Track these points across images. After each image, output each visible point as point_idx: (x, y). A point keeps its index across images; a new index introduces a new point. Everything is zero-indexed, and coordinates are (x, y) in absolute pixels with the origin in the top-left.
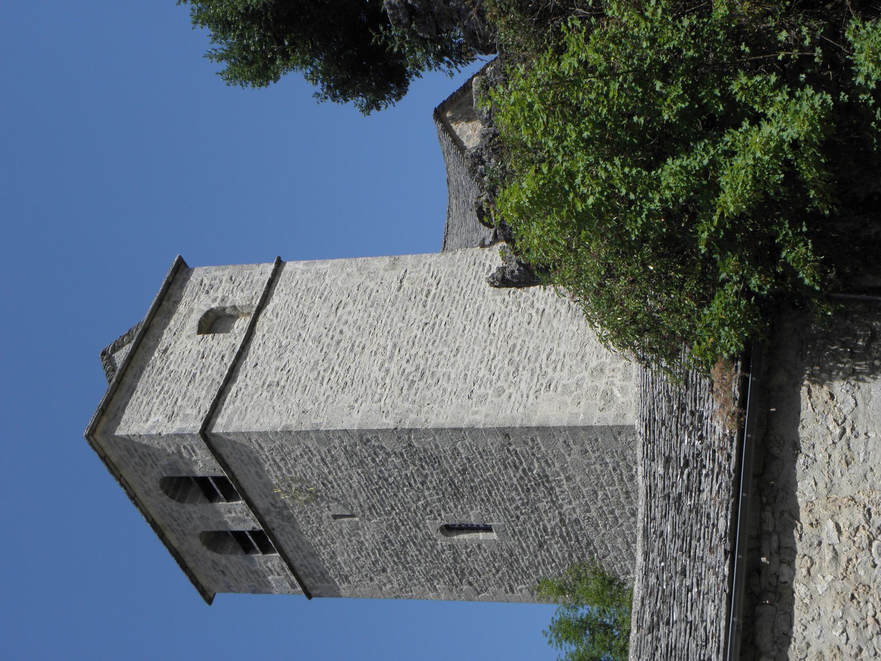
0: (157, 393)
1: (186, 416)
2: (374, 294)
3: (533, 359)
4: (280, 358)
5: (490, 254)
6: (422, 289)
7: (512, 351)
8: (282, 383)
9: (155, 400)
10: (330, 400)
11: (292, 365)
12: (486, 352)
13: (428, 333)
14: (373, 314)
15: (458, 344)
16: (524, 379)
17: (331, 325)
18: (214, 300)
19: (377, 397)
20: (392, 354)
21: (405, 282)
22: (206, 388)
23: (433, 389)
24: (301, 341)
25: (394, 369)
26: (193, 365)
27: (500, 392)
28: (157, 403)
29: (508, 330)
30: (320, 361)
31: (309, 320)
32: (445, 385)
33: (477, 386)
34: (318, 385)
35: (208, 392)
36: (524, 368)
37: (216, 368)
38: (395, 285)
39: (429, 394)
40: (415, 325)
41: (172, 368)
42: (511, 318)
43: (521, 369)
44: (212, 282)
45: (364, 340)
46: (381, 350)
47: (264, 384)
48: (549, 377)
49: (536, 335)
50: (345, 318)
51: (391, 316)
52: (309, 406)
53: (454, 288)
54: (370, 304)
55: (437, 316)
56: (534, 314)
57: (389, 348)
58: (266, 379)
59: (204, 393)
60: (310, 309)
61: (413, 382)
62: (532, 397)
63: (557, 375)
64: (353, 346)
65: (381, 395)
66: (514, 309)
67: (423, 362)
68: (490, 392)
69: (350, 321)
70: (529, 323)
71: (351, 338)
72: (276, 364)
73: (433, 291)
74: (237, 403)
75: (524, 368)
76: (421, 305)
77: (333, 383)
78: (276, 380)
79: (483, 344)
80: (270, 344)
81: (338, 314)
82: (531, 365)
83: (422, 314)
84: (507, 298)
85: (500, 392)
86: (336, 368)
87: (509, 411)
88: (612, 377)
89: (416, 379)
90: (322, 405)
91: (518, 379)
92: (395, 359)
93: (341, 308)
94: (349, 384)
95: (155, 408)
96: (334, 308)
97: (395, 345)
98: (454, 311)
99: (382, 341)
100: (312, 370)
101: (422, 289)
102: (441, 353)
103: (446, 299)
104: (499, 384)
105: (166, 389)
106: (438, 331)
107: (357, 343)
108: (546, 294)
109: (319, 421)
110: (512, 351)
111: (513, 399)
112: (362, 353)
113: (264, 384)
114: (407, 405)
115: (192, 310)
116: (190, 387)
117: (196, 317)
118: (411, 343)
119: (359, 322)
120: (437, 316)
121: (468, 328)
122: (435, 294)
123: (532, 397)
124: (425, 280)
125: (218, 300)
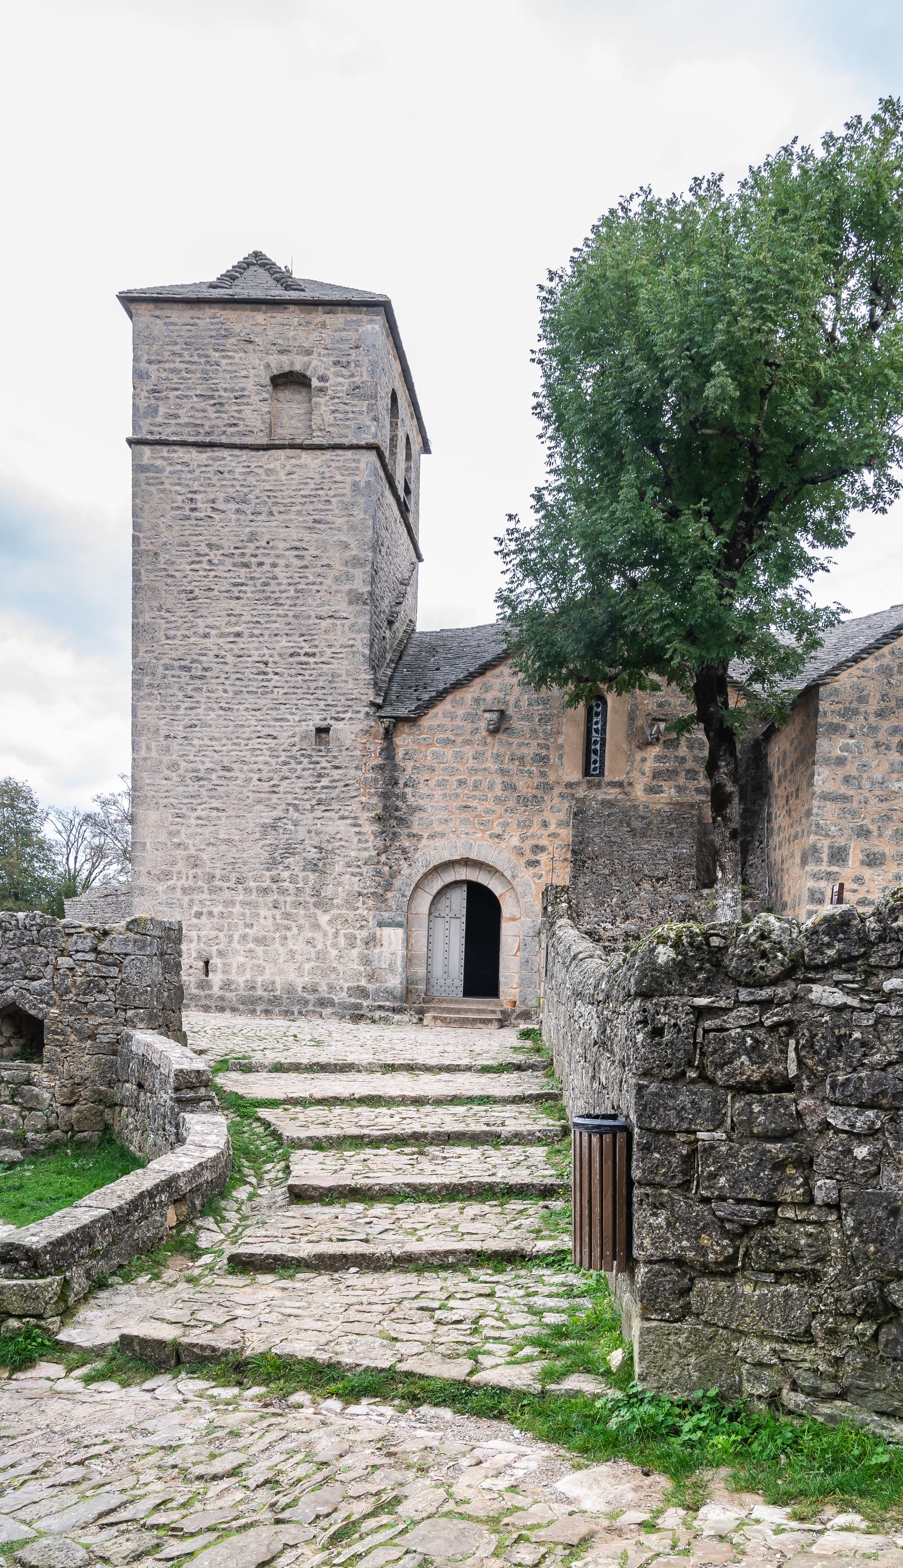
0: (187, 359)
1: (156, 411)
2: (315, 587)
3: (212, 793)
4: (227, 500)
5: (362, 715)
6: (316, 646)
7: (225, 768)
9: (178, 359)
10: (169, 580)
12: (224, 741)
13: (254, 670)
14: (284, 595)
15: (236, 707)
16: (187, 789)
17: (272, 548)
19: (171, 633)
20: (229, 634)
21: (329, 621)
22: (191, 420)
23: (180, 695)
24: (251, 517)
25: (208, 642)
26: (226, 390)
27: (174, 766)
28: (172, 366)
30: (221, 552)
31: (283, 517)
32: (183, 706)
33: (181, 741)
34: (190, 560)
35: (187, 425)
36: (201, 786)
37: (219, 422)
38: (324, 611)
40: (266, 651)
41: (224, 362)
42: (268, 759)
43: (201, 783)
44: (353, 365)
45: (249, 595)
46: (233, 619)
47: (195, 492)
48: (188, 813)
49: (245, 790)
50: (282, 562)
51: (279, 619)
52: (164, 557)
54: (300, 587)
55: (276, 674)
56: (272, 783)
57: (237, 629)
58: (201, 492)
59: (186, 420)
60: (299, 513)
61: (189, 669)
63: (193, 821)
64: (242, 584)
65: (174, 637)
67: (214, 674)
68: (174, 757)
69: (277, 571)
70: (259, 780)
71: (252, 578)
72: (221, 496)
73: (311, 660)
74: (169, 469)
75: (201, 786)
76: (292, 650)
78: (199, 505)
79: (233, 736)
80: (251, 479)
81: (287, 553)
82: (205, 793)
83: (280, 655)
84: (297, 748)
85: (174, 766)
86: (212, 574)
87: (148, 781)
88: (187, 878)
89: (193, 672)
90: (164, 573)
91: (189, 782)
92: (221, 641)
93: (296, 553)
94: (190, 596)
95: (166, 366)
96: (297, 544)
97: (238, 635)
98: (282, 691)
100: (210, 546)
101: (316, 646)
102: (225, 691)
103: (300, 678)
104: (183, 765)
105: (194, 367)
106: (257, 680)
107: (243, 588)
108: (298, 790)
110: (225, 768)
111: (164, 782)
112: (231, 598)
113: (195, 492)
114: (161, 670)
115: (309, 352)
116: (195, 399)
117: (298, 364)
118: (241, 653)
119: (273, 582)
120: (276, 674)
121: (258, 713)
122: (306, 663)
123: (165, 801)
124: (330, 646)
125: (322, 384)
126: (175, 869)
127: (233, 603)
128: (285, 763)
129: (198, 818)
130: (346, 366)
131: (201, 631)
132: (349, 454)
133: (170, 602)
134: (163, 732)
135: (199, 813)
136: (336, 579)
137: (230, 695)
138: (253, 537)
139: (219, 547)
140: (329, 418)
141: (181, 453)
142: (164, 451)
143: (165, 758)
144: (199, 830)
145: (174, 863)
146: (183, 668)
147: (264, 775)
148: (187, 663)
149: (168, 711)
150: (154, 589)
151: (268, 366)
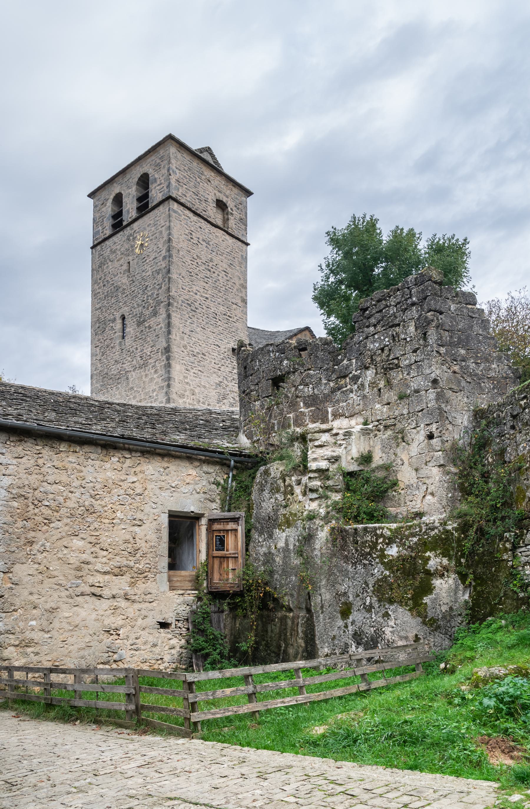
1: (178, 189)
4: (204, 240)
7: (203, 354)
8: (192, 240)
11: (200, 246)
18: (232, 209)
19: (184, 287)
25: (197, 297)
27: (185, 347)
29: (212, 353)
31: (220, 257)
35: (189, 202)
38: (234, 301)
39: (184, 313)
52: (181, 253)
53: (231, 330)
59: (189, 199)
61: (190, 306)
62: (183, 362)
63: (192, 374)
65: (185, 290)
66: (222, 357)
69: (220, 278)
72: (201, 238)
77: (191, 266)
80: (210, 236)
85: (185, 347)
97: (207, 298)
99: (209, 292)
104: (188, 347)
109: (174, 257)
110: (203, 354)
114: (180, 302)
115: (227, 197)
117: (225, 200)
123: (183, 362)
126: (186, 394)
127: (205, 284)
128: (223, 359)
129: (194, 373)
130: (238, 209)
131: (194, 291)
132: (240, 243)
133: (183, 274)
134: (181, 330)
135: (194, 371)
136: (237, 290)
137: (204, 323)
138: (211, 260)
139: (200, 259)
140: (234, 226)
141: (187, 212)
142: (182, 208)
143: (182, 342)
144: (194, 379)
145: (185, 391)
146: (188, 304)
147: (217, 362)
148: (189, 303)
149: (183, 321)
150: (178, 265)
151: (215, 194)
